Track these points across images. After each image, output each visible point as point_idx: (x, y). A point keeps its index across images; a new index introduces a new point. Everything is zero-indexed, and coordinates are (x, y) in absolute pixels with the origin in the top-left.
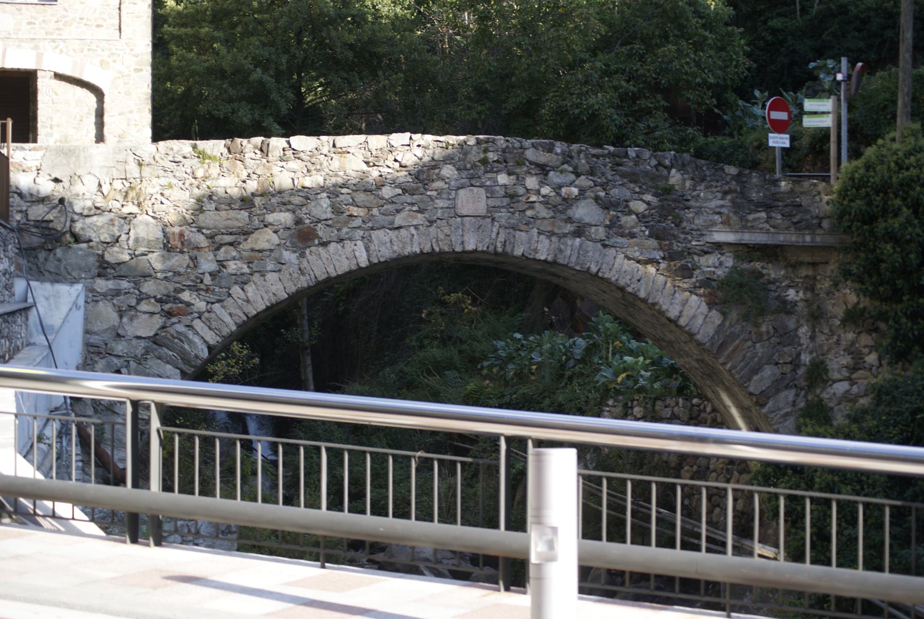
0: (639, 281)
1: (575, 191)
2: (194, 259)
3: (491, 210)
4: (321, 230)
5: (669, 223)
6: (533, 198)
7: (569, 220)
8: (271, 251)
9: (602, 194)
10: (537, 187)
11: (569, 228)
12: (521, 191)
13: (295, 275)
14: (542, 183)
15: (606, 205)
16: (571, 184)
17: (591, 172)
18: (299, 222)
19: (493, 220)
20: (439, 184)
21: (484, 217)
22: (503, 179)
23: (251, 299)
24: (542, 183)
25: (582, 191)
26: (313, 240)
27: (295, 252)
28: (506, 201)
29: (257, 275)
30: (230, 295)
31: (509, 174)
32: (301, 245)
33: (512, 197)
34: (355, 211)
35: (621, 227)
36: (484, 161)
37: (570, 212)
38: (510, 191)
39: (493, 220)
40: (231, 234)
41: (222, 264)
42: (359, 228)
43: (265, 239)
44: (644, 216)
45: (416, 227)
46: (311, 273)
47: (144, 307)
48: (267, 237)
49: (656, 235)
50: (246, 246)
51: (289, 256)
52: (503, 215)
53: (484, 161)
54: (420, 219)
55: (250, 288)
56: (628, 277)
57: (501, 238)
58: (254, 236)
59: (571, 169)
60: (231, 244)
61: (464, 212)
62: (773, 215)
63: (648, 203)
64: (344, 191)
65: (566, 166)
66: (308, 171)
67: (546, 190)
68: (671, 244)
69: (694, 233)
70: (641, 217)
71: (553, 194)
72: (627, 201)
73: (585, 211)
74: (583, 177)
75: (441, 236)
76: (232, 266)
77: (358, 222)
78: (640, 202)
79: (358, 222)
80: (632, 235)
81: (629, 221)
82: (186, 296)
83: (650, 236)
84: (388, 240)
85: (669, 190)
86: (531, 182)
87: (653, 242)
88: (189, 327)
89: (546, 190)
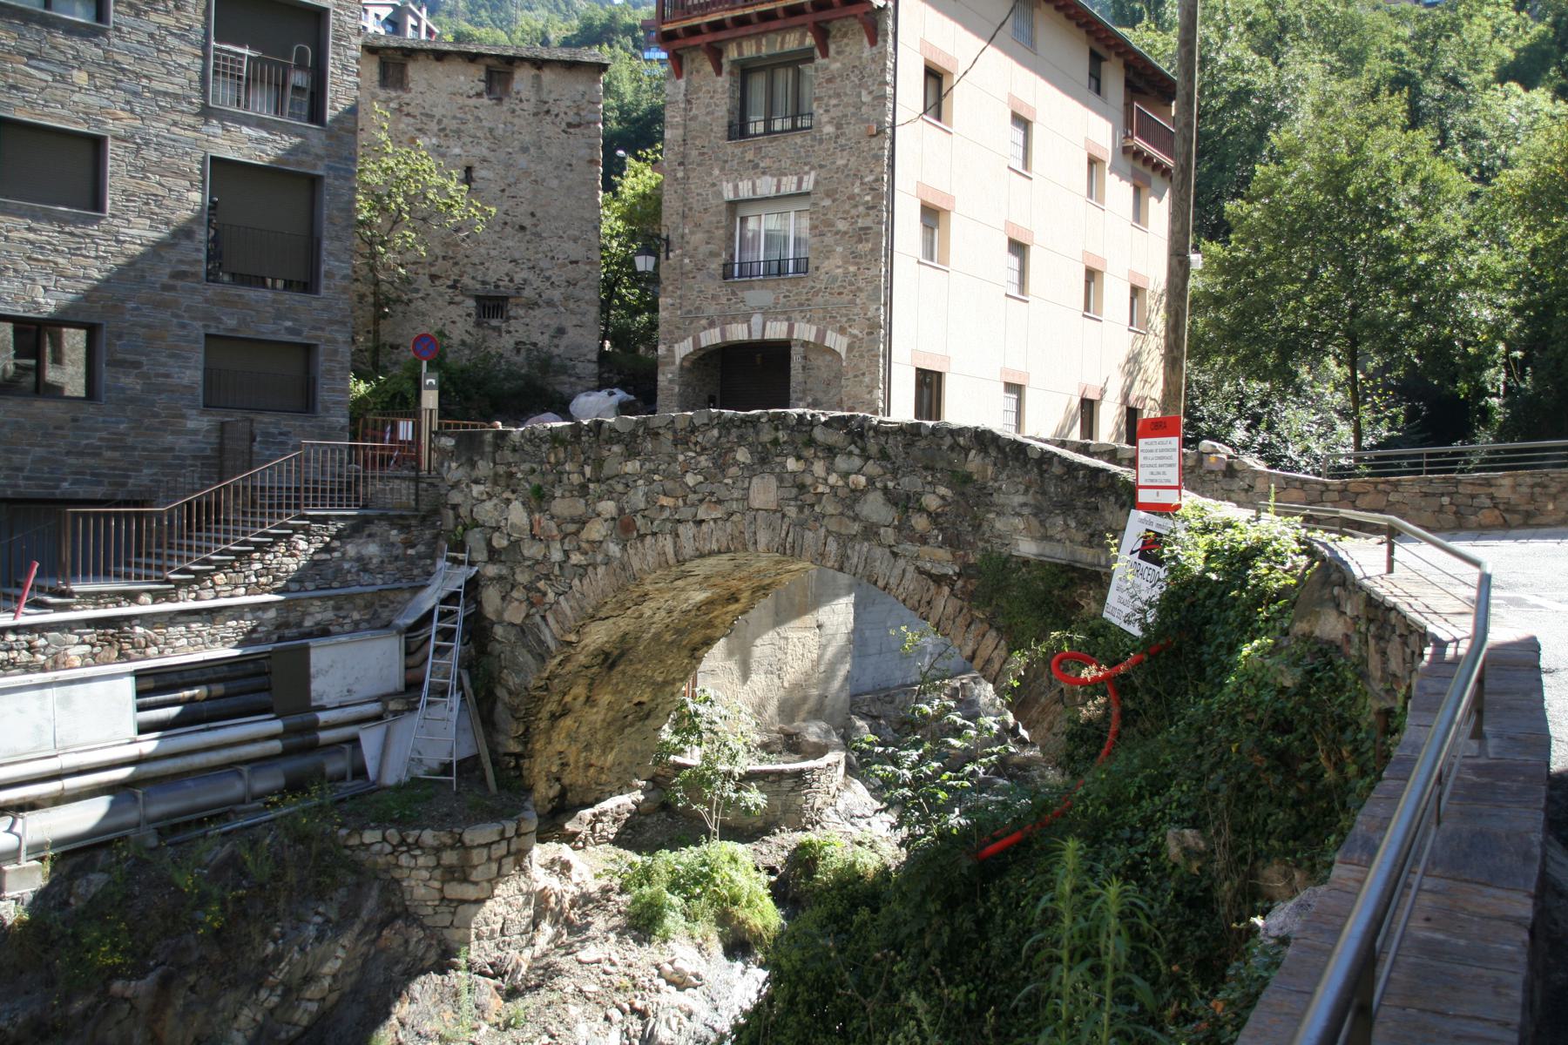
0: (929, 603)
1: (862, 480)
2: (548, 547)
3: (783, 501)
5: (966, 527)
6: (820, 489)
9: (891, 485)
10: (824, 475)
11: (856, 528)
12: (808, 480)
14: (829, 471)
15: (891, 498)
16: (859, 472)
17: (884, 455)
18: (621, 511)
19: (784, 516)
20: (733, 471)
21: (775, 511)
22: (792, 464)
24: (829, 471)
25: (871, 481)
28: (795, 491)
31: (799, 458)
33: (802, 487)
34: (665, 501)
35: (912, 529)
36: (775, 442)
37: (857, 508)
38: (799, 480)
39: (784, 516)
41: (566, 553)
43: (596, 530)
44: (938, 515)
45: (715, 520)
47: (515, 594)
49: (953, 542)
50: (584, 535)
51: (614, 549)
52: (792, 511)
53: (775, 442)
54: (718, 513)
55: (586, 581)
56: (917, 597)
57: (790, 539)
59: (857, 451)
63: (943, 498)
65: (852, 447)
67: (833, 479)
68: (966, 554)
69: (995, 540)
70: (934, 517)
71: (841, 483)
72: (921, 494)
73: (875, 508)
74: (871, 462)
76: (576, 558)
77: (666, 514)
78: (933, 497)
79: (666, 514)
80: (923, 540)
81: (920, 523)
82: (541, 584)
83: (944, 542)
85: (967, 478)
86: (819, 468)
87: (944, 554)
88: (543, 617)
89: (833, 479)
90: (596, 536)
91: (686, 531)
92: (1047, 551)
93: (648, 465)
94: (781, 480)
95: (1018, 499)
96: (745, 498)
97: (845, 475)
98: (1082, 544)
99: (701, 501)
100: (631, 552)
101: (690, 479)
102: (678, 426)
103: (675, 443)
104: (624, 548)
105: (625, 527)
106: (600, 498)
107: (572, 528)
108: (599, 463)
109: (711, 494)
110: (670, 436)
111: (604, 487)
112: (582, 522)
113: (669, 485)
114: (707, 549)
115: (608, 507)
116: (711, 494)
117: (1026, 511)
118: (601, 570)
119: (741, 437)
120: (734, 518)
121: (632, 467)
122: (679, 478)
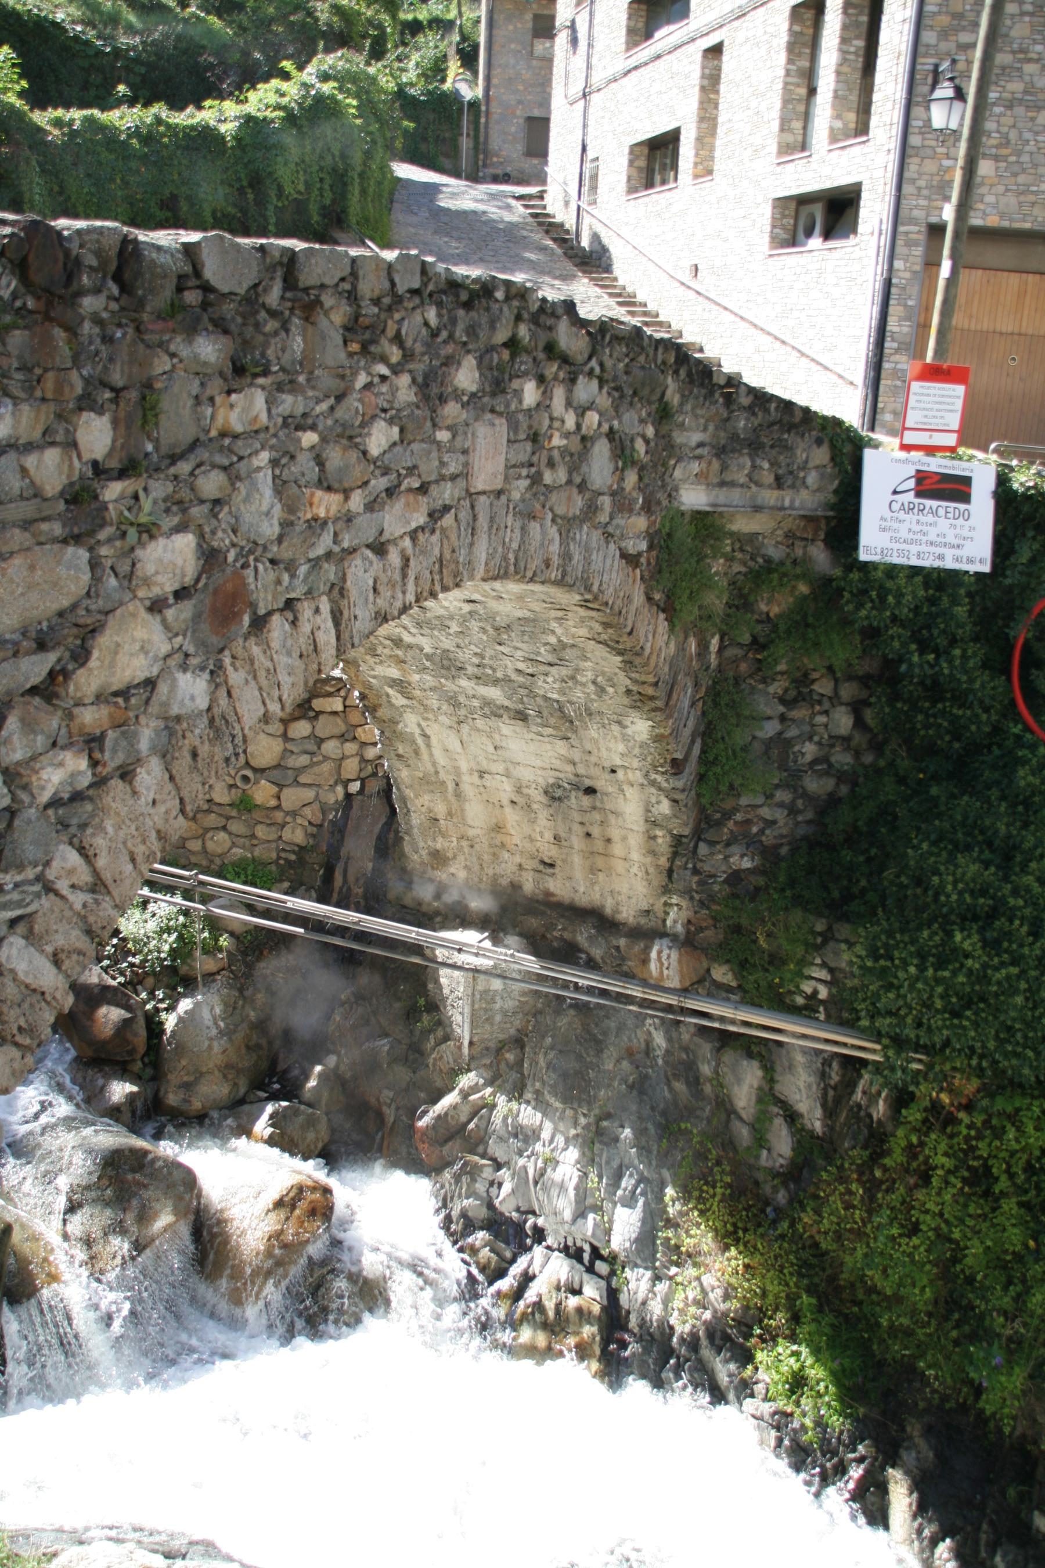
4: (263, 586)
7: (582, 487)
8: (150, 684)
11: (579, 502)
13: (204, 750)
14: (569, 404)
18: (210, 557)
20: (452, 410)
22: (530, 393)
23: (107, 876)
26: (236, 616)
27: (203, 669)
28: (529, 446)
29: (116, 784)
30: (49, 889)
32: (215, 640)
34: (325, 504)
36: (512, 344)
40: (42, 646)
42: (329, 555)
45: (413, 535)
46: (237, 731)
48: (140, 633)
50: (88, 680)
51: (191, 690)
57: (515, 545)
58: (104, 641)
60: (33, 691)
61: (480, 483)
62: (758, 462)
64: (309, 438)
66: (239, 370)
73: (600, 467)
75: (447, 555)
77: (325, 543)
79: (325, 543)
84: (371, 582)
90: (134, 668)
91: (361, 573)
92: (722, 499)
93: (288, 403)
94: (513, 426)
95: (696, 437)
96: (464, 474)
97: (581, 412)
98: (770, 487)
99: (390, 492)
100: (236, 677)
101: (379, 438)
102: (370, 286)
103: (350, 329)
104: (216, 673)
105: (221, 609)
106: (149, 531)
107: (35, 668)
108: (139, 406)
109: (412, 470)
110: (338, 314)
111: (160, 488)
112: (72, 636)
113: (335, 457)
114: (398, 604)
115: (171, 557)
116: (412, 470)
117: (704, 451)
118: (150, 777)
119: (472, 330)
120: (448, 520)
121: (248, 407)
122: (351, 437)
